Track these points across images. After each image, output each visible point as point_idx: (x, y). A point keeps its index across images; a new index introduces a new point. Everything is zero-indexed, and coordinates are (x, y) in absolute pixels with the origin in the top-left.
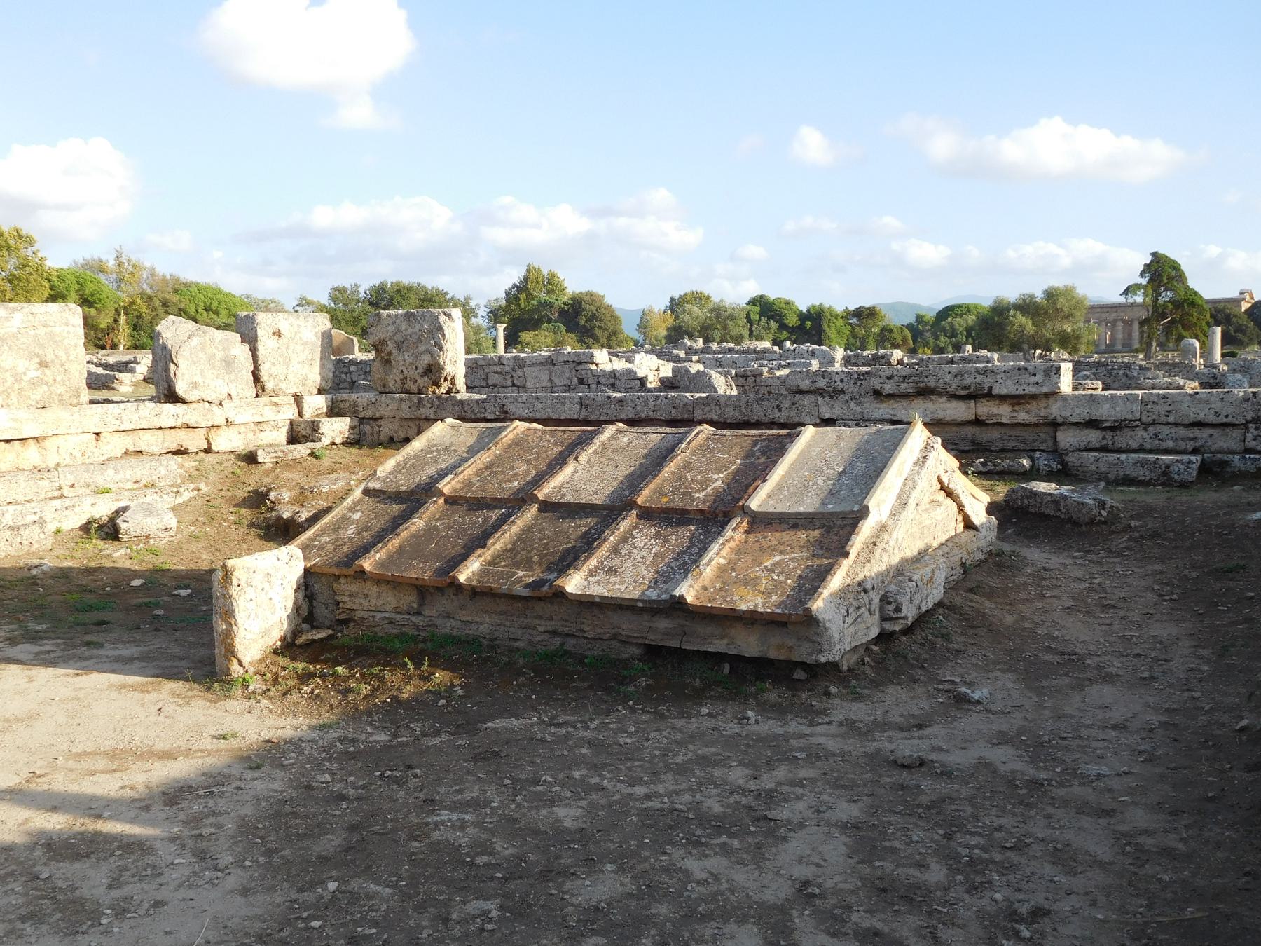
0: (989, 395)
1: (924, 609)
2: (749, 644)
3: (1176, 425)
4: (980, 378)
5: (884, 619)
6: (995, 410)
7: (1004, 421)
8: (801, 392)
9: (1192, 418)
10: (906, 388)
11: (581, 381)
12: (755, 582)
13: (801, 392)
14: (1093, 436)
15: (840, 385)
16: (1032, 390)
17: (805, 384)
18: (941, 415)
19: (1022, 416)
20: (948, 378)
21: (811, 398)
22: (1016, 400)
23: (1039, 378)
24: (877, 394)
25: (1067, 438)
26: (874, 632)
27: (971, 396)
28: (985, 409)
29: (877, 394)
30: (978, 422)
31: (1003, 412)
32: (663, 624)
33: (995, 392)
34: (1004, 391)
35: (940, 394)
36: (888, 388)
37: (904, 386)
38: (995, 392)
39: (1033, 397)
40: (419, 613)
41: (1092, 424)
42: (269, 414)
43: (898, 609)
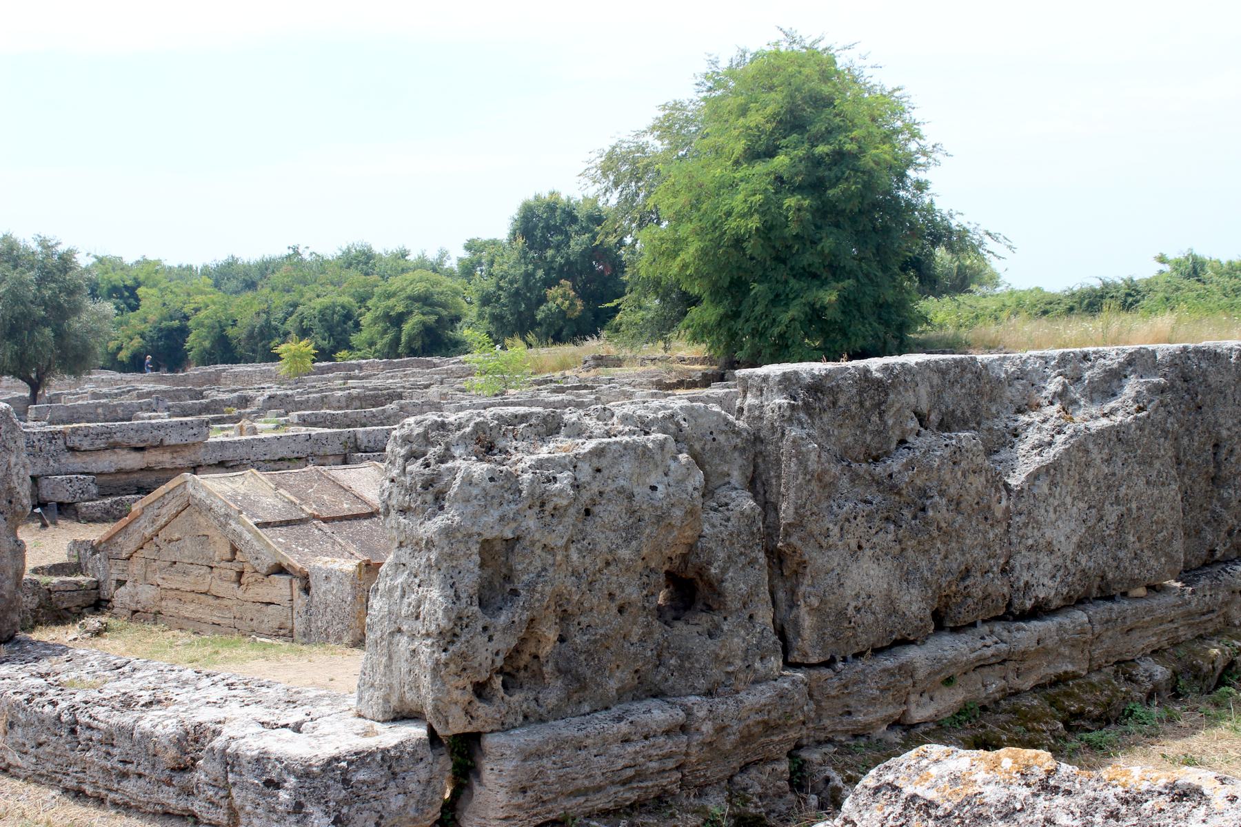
3: (270, 461)
4: (155, 432)
6: (160, 459)
7: (168, 466)
9: (280, 456)
10: (100, 443)
16: (191, 440)
20: (132, 433)
22: (174, 449)
23: (195, 431)
24: (72, 450)
30: (149, 469)
33: (166, 443)
34: (173, 442)
36: (86, 445)
38: (166, 443)
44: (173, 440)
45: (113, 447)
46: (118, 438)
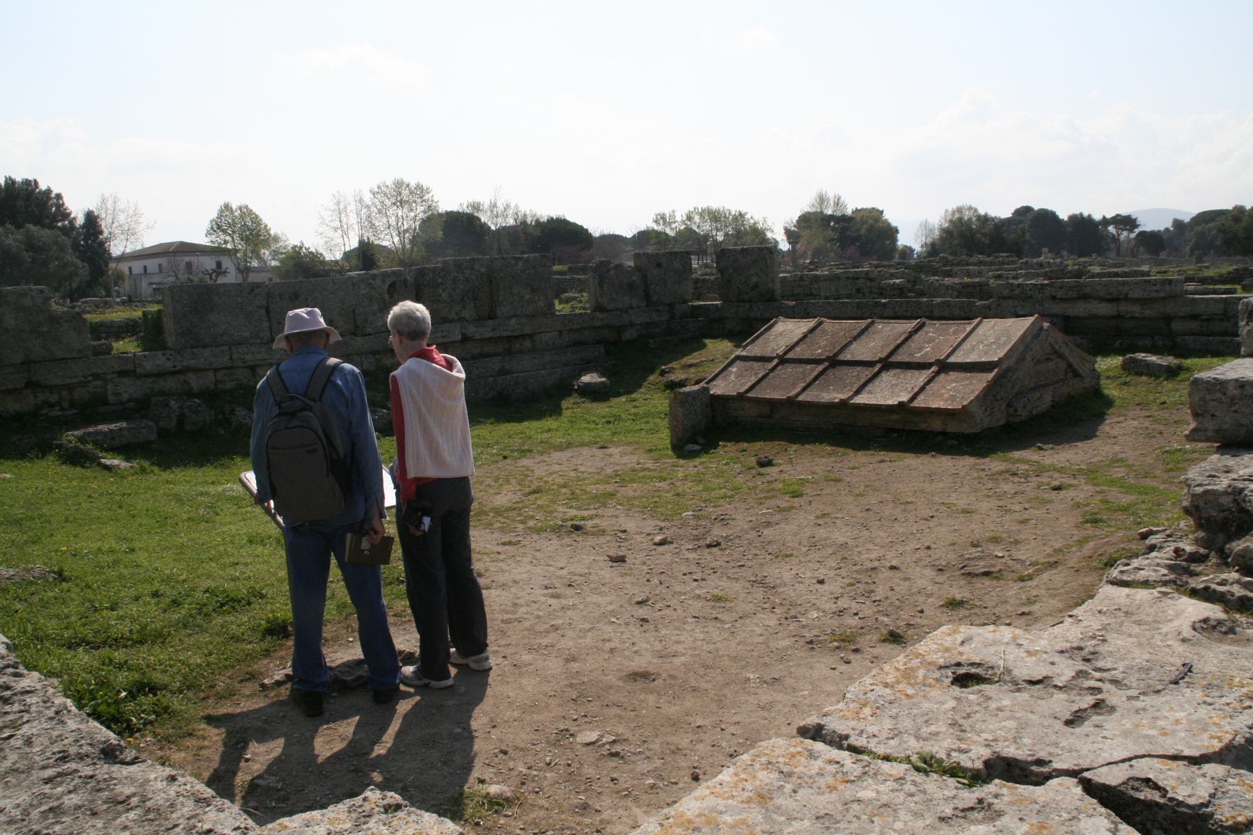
0: (1126, 299)
1: (1034, 412)
2: (936, 425)
5: (1009, 415)
8: (1005, 298)
11: (858, 291)
12: (941, 395)
13: (1005, 298)
14: (1195, 325)
15: (1030, 293)
16: (1155, 295)
17: (1006, 292)
18: (1095, 312)
19: (1148, 312)
20: (1099, 288)
21: (1010, 302)
23: (1158, 287)
24: (1054, 298)
25: (1176, 326)
26: (1002, 422)
27: (1115, 300)
28: (1124, 308)
29: (1054, 298)
30: (1119, 316)
31: (1136, 310)
32: (895, 417)
34: (1136, 296)
35: (1095, 298)
36: (1060, 294)
37: (1070, 293)
39: (1155, 300)
40: (770, 417)
41: (1194, 317)
42: (655, 317)
43: (1016, 411)
44: (1137, 293)
45: (1085, 297)
46: (1087, 290)
